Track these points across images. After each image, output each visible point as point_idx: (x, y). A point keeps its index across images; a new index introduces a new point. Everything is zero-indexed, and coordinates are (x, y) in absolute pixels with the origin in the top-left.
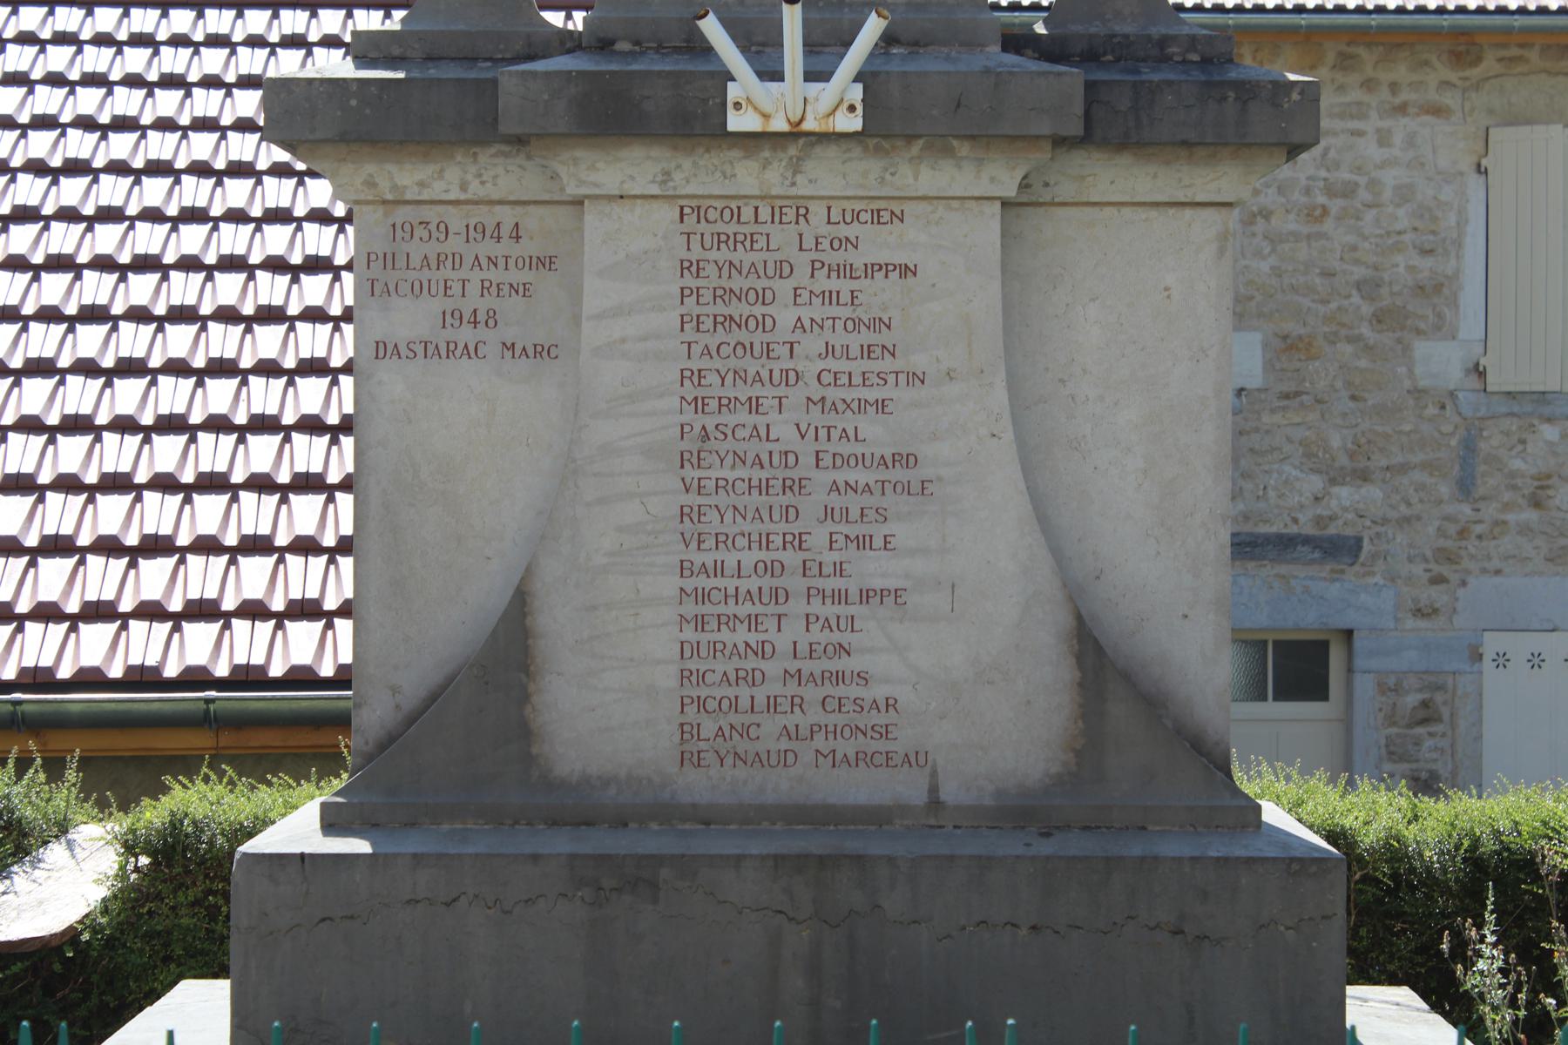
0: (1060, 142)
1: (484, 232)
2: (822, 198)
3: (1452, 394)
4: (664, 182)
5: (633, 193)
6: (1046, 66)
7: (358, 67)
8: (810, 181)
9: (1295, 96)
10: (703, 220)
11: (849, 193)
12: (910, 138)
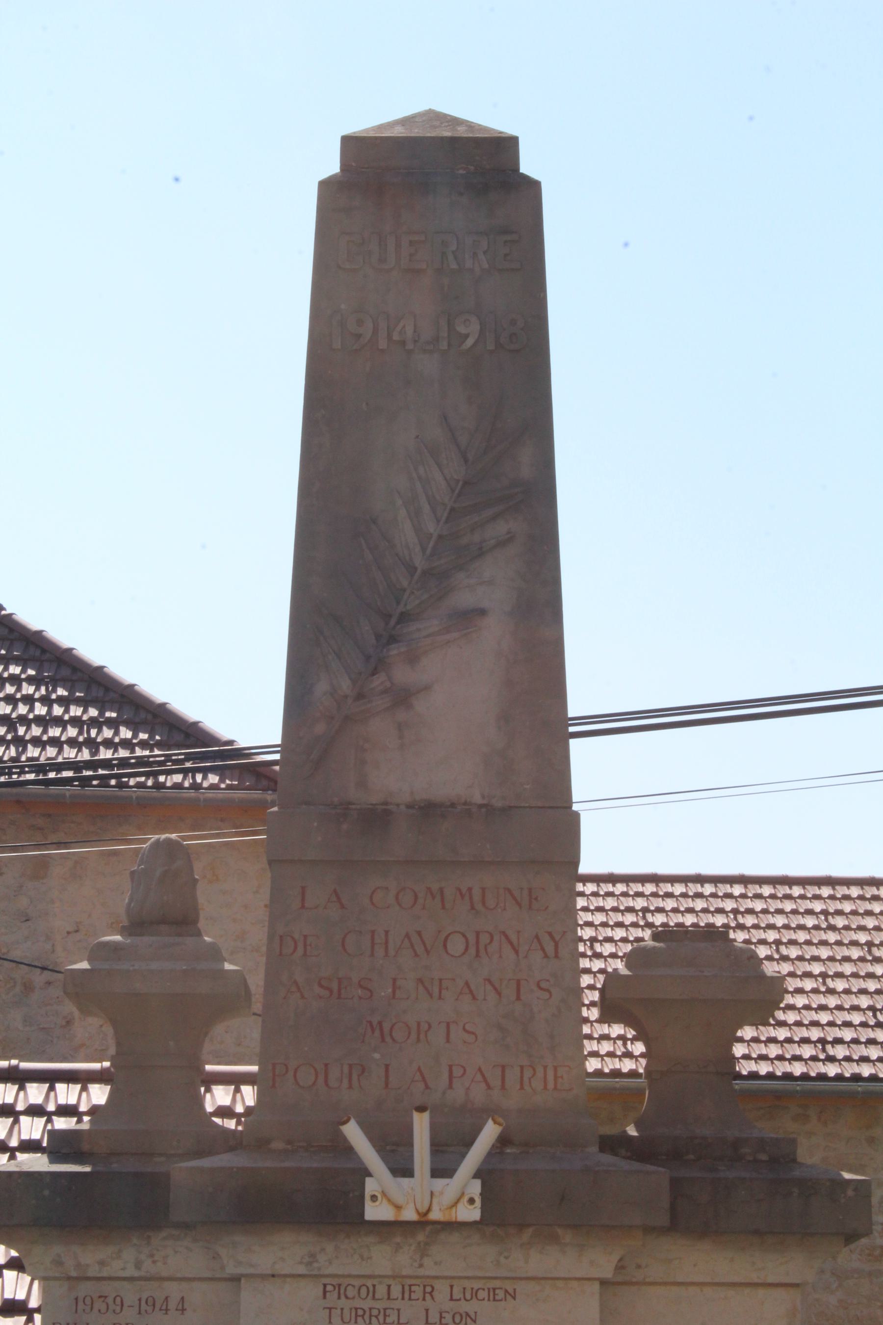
0: (648, 1230)
1: (154, 1305)
2: (446, 1278)
4: (309, 1264)
5: (283, 1272)
6: (636, 1166)
7: (52, 1161)
8: (436, 1263)
9: (850, 1193)
10: (343, 1296)
11: (470, 1273)
12: (521, 1227)
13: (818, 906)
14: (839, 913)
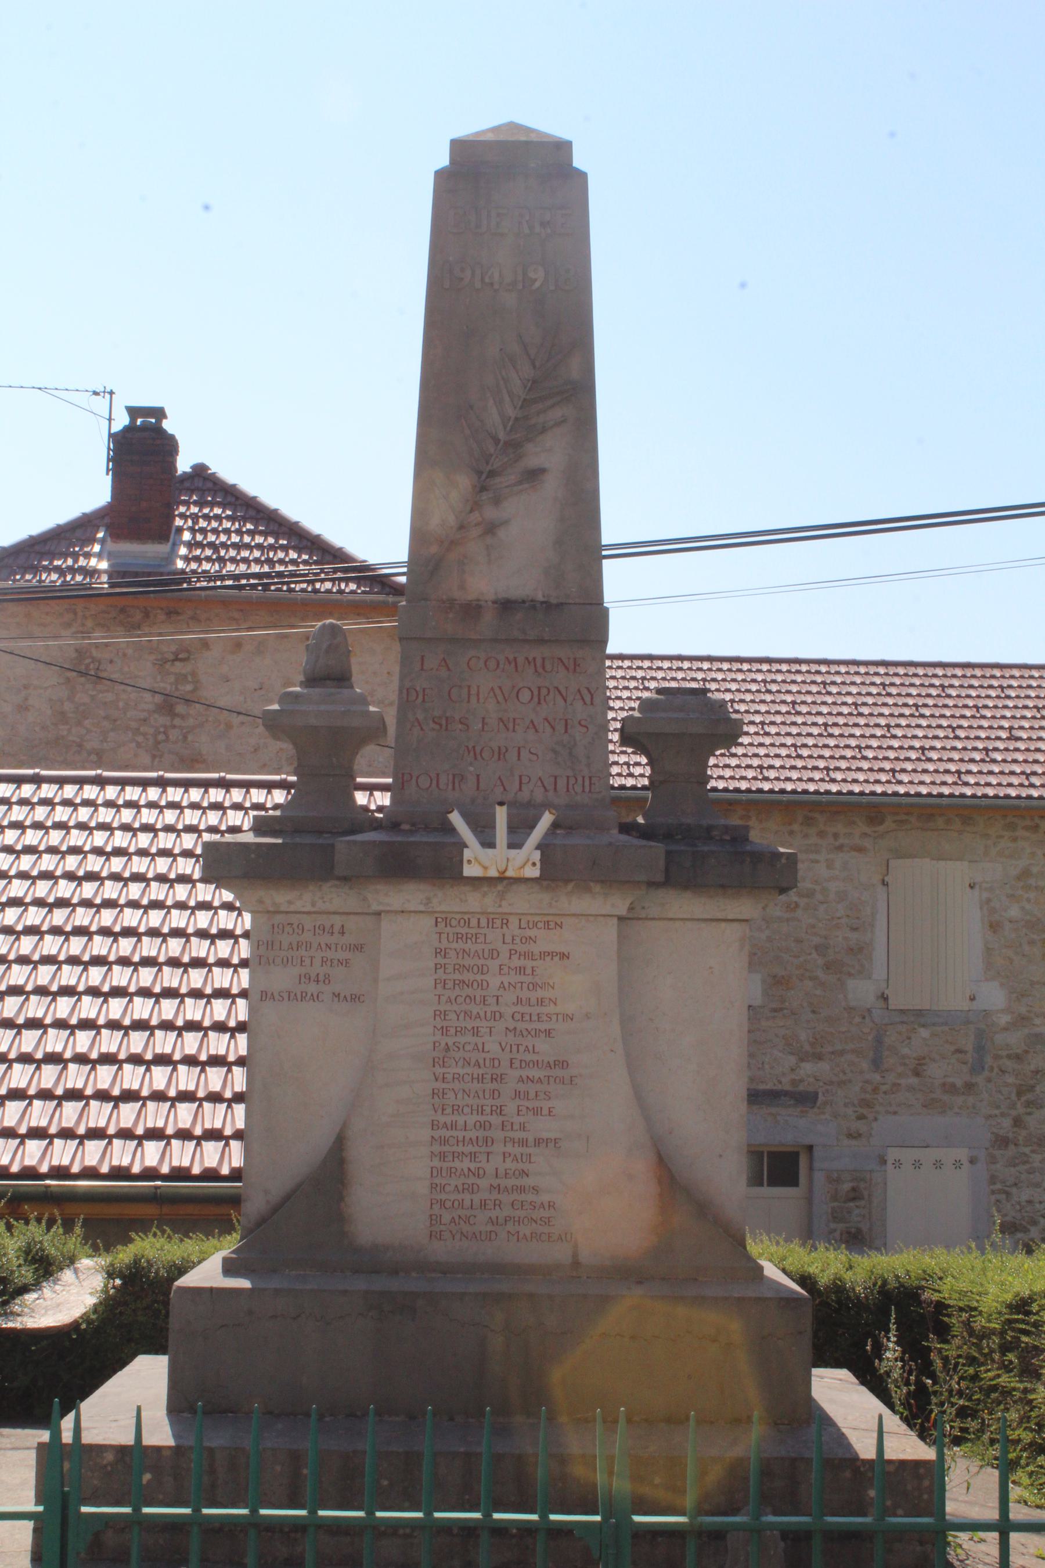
0: (652, 884)
2: (517, 914)
3: (869, 1010)
6: (644, 842)
9: (783, 861)
10: (448, 925)
11: (532, 911)
12: (567, 881)
13: (759, 677)
14: (774, 681)
